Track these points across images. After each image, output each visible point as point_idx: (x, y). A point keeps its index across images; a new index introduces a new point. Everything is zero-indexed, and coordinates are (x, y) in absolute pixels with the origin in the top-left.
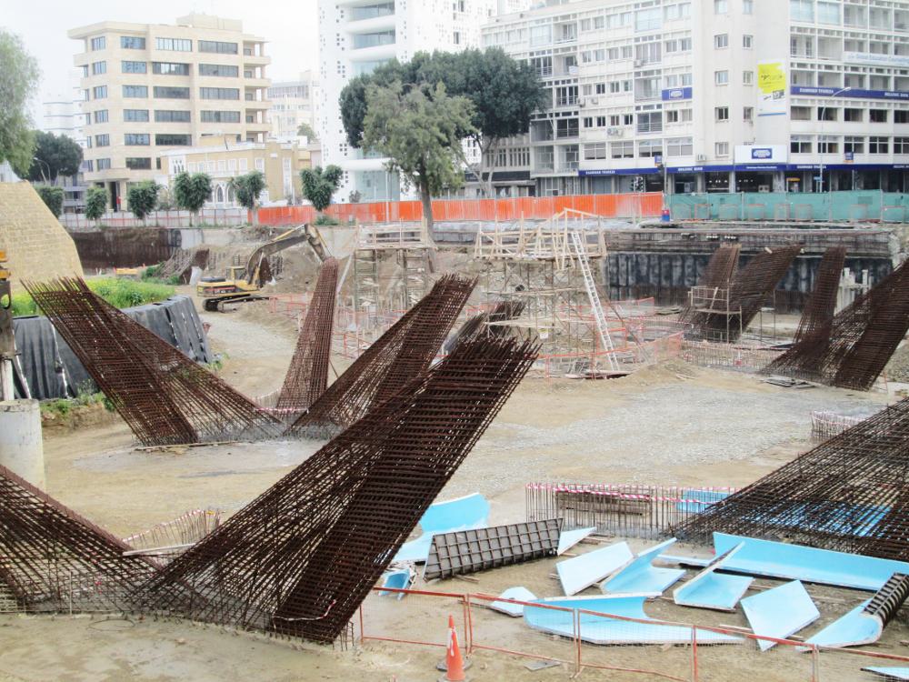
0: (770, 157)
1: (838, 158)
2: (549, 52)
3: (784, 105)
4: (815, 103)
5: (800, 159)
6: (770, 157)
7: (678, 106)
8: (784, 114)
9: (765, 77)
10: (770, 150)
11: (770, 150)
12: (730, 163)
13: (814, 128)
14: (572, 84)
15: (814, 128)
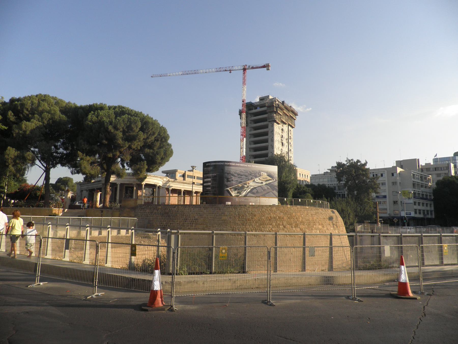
0: (410, 215)
1: (421, 216)
2: (335, 184)
3: (412, 201)
4: (417, 201)
5: (418, 216)
6: (410, 215)
7: (382, 200)
8: (412, 203)
9: (405, 193)
10: (410, 213)
11: (410, 213)
12: (400, 216)
13: (417, 207)
14: (343, 193)
15: (417, 207)
